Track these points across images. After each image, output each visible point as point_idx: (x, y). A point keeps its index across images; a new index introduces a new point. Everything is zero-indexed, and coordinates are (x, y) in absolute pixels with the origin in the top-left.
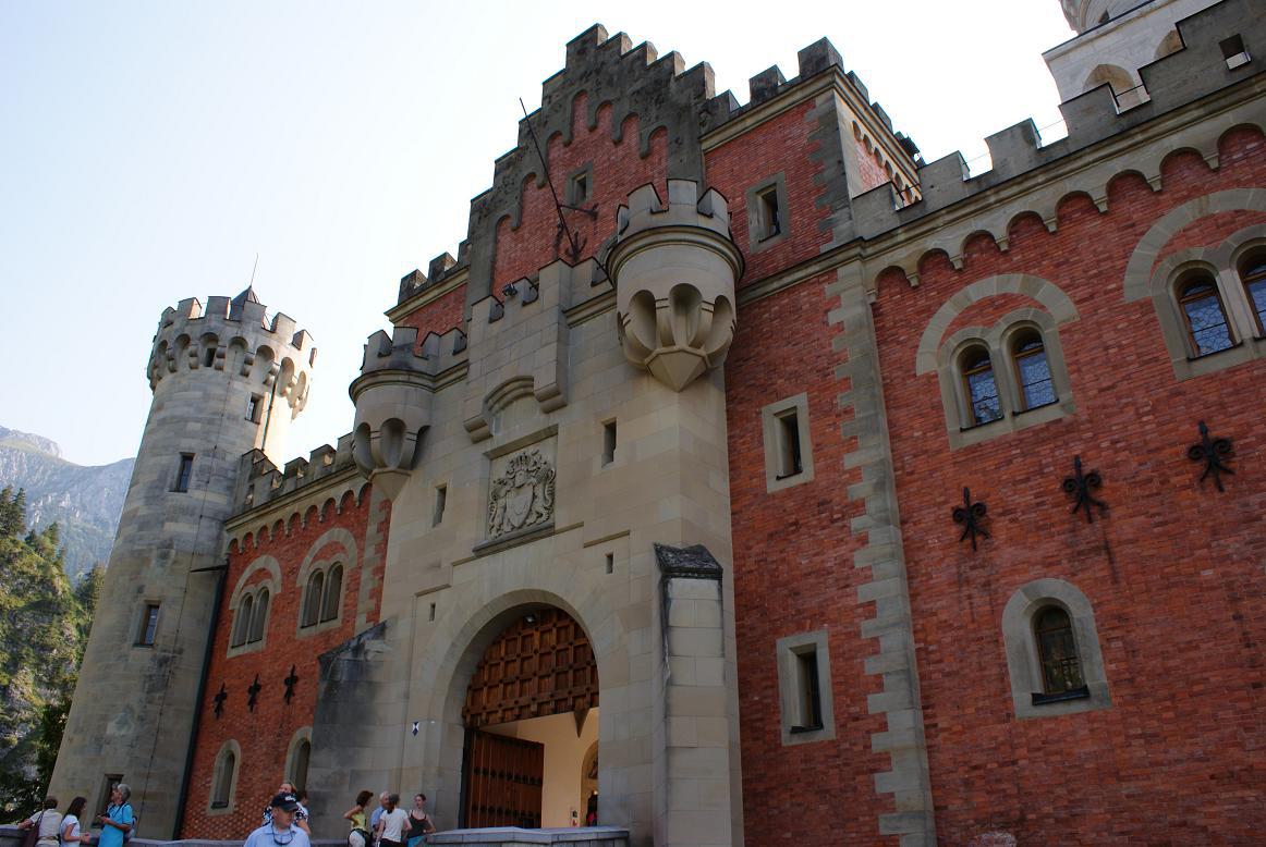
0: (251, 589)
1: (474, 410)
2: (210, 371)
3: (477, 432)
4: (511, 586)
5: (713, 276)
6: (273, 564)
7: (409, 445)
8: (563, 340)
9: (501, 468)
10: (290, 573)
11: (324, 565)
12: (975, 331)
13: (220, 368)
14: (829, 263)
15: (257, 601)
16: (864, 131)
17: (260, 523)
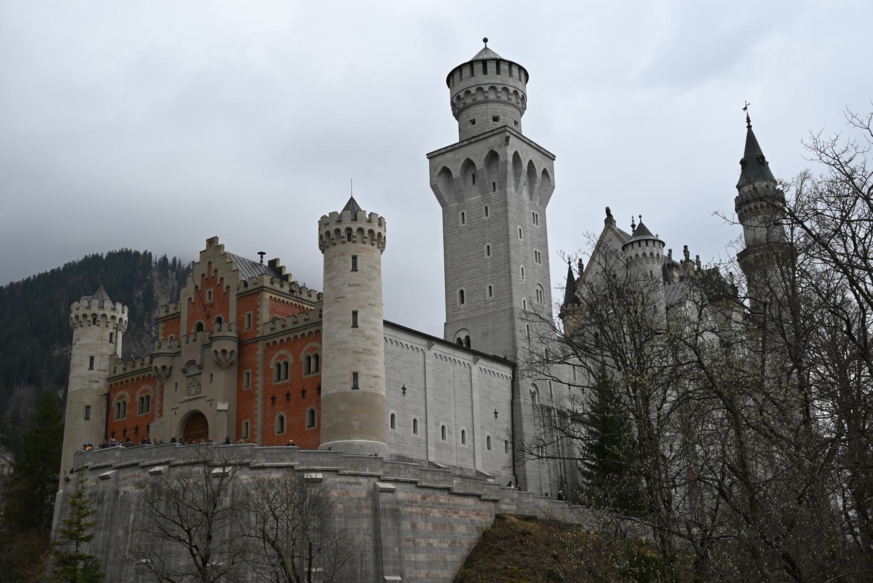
0: (119, 401)
1: (183, 366)
2: (95, 326)
3: (184, 371)
4: (192, 408)
5: (231, 346)
6: (127, 394)
7: (167, 372)
8: (202, 352)
9: (190, 380)
10: (133, 397)
11: (144, 396)
12: (279, 361)
13: (98, 325)
14: (257, 340)
15: (122, 405)
16: (274, 296)
17: (120, 380)
